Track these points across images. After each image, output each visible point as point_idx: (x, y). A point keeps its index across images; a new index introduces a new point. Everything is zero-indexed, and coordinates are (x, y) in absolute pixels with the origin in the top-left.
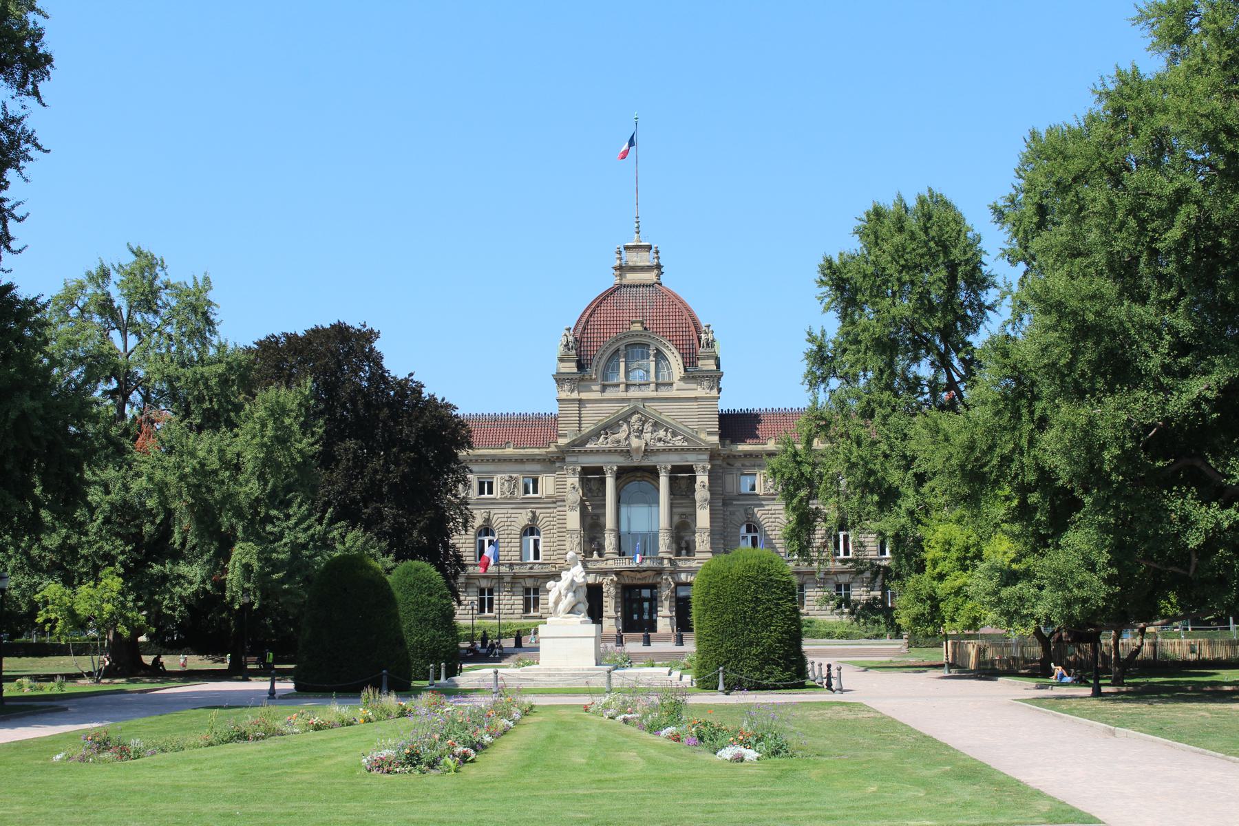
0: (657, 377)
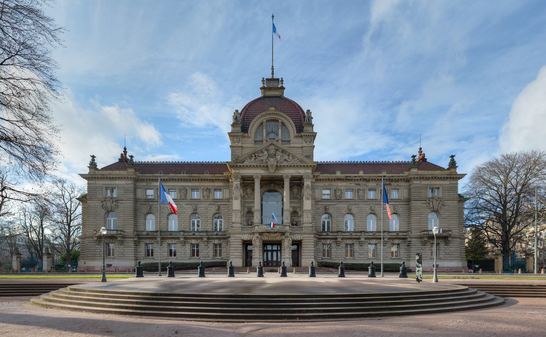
0: (282, 137)
